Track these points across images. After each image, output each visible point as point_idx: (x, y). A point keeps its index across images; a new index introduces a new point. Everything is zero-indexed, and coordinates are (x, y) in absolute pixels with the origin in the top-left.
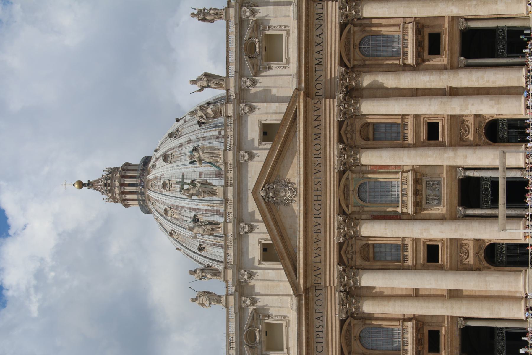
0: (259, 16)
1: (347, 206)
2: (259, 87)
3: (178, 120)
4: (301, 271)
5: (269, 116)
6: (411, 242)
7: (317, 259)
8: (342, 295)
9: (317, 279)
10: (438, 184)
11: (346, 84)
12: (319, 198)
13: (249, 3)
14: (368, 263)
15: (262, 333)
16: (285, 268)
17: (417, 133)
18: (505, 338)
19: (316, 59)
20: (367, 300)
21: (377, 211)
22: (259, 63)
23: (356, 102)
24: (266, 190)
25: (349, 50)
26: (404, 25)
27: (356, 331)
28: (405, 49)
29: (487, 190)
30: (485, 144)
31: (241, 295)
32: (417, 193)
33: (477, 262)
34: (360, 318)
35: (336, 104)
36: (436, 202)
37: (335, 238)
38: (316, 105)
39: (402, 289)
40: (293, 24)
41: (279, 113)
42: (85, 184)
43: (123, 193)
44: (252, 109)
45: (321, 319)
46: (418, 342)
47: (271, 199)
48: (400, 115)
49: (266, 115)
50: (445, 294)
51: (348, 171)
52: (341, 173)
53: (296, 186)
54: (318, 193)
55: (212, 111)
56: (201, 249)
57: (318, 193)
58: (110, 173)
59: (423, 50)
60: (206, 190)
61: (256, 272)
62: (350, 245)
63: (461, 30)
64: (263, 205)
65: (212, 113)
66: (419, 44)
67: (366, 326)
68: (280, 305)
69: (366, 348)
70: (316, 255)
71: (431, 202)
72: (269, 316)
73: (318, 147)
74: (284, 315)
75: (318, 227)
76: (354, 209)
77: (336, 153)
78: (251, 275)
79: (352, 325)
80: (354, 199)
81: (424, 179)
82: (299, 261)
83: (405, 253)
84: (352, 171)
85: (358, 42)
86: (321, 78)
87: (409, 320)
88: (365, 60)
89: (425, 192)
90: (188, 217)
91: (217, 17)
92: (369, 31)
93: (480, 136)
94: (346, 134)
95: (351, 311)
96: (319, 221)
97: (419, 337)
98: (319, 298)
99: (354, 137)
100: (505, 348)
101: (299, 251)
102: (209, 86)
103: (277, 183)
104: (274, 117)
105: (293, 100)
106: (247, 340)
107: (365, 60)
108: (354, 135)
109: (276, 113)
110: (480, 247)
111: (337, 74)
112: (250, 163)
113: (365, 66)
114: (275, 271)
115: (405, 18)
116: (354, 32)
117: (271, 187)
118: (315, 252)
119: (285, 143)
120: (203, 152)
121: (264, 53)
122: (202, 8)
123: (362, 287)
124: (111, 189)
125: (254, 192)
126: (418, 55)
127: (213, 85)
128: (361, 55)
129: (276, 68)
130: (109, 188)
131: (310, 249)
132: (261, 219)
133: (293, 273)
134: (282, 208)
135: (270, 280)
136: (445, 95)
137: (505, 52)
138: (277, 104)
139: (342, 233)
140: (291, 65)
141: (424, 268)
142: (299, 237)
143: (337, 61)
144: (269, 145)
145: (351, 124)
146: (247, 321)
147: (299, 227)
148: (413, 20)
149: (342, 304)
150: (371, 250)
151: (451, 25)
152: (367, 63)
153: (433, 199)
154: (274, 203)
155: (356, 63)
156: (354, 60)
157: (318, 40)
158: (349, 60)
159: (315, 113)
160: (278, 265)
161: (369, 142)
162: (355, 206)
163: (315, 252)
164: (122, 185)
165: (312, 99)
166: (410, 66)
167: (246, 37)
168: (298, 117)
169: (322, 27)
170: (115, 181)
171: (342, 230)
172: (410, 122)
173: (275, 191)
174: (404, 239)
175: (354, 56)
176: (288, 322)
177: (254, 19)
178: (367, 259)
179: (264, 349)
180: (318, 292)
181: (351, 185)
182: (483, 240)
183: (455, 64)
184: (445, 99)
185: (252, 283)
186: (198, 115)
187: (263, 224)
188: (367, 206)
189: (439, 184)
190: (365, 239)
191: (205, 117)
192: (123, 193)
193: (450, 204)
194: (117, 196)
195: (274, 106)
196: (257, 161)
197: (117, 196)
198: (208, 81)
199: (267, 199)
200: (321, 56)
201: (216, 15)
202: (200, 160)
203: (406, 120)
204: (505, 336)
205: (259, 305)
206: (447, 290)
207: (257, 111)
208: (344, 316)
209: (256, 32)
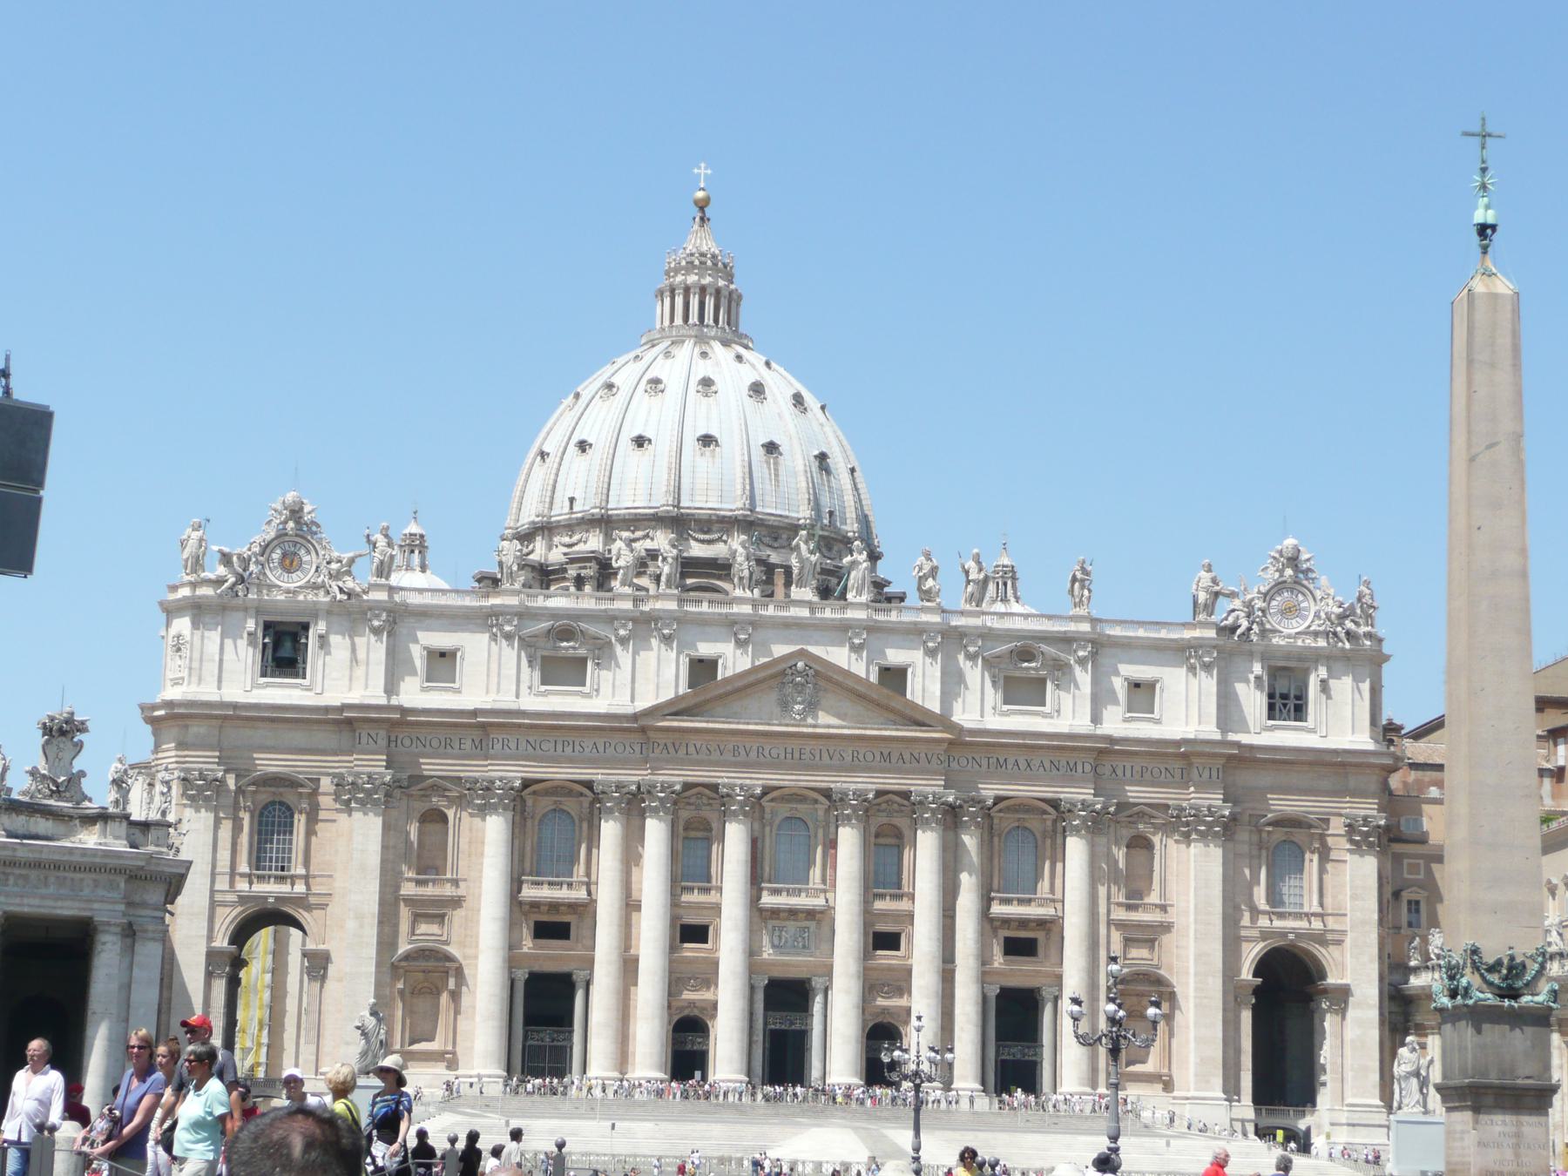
0: (1078, 670)
1: (772, 800)
2: (964, 664)
3: (823, 408)
4: (675, 724)
5: (920, 679)
6: (714, 901)
7: (692, 749)
8: (634, 787)
9: (661, 747)
10: (804, 947)
11: (965, 806)
12: (789, 756)
13: (1097, 653)
14: (681, 828)
15: (571, 651)
16: (678, 699)
17: (884, 915)
18: (555, 1043)
19: (1005, 760)
20: (622, 824)
21: (763, 847)
22: (1002, 666)
23: (938, 822)
24: (805, 670)
25: (1017, 811)
26: (1053, 901)
27: (570, 805)
28: (1015, 902)
29: (792, 1024)
30: (864, 1021)
31: (635, 620)
32: (793, 913)
33: (680, 1004)
34: (591, 813)
35: (937, 789)
36: (776, 942)
37: (726, 780)
38: (935, 757)
39: (641, 883)
40: (1061, 725)
41: (923, 696)
42: (703, 212)
43: (687, 290)
44: (931, 653)
45: (595, 750)
46: (554, 906)
47: (791, 678)
48: (914, 889)
49: (921, 675)
50: (632, 951)
51: (828, 803)
52: (827, 793)
53: (810, 721)
54: (797, 755)
55: (930, 588)
56: (583, 446)
57: (797, 755)
58: (725, 266)
59: (1013, 930)
60: (806, 571)
61: (672, 649)
62: (711, 801)
63: (1039, 989)
64: (784, 666)
65: (927, 586)
66: (1023, 923)
67: (577, 821)
68: (617, 683)
69: (540, 821)
70: (698, 747)
71: (777, 933)
72: (598, 664)
73: (869, 757)
74: (601, 690)
75: (743, 752)
76: (768, 810)
77: (860, 786)
78: (667, 640)
79: (581, 799)
80: (784, 810)
81: (812, 925)
82: (692, 721)
83: (696, 891)
84: (828, 810)
85: (1027, 825)
86: (977, 766)
87: (589, 893)
88: (1000, 836)
89: (792, 926)
90: (645, 425)
91: (1077, 600)
92: (1044, 842)
93: (878, 1015)
94: (887, 802)
95: (605, 800)
96: (753, 755)
97: (562, 908)
98: (628, 748)
99: (881, 814)
100: (540, 1043)
101: (707, 722)
102: (968, 582)
103: (815, 688)
104: (918, 687)
105: (944, 721)
106: (560, 626)
107: (1000, 836)
108: (885, 814)
109: (924, 690)
110: (703, 1009)
111: (984, 792)
112: (846, 650)
113: (991, 836)
114: (674, 678)
115: (1063, 902)
116: (1045, 820)
117: (809, 680)
118: (704, 746)
119: (878, 705)
120: (866, 569)
121: (1017, 674)
122: (1093, 577)
123: (645, 819)
124: (695, 267)
125: (802, 654)
126: (1006, 922)
127: (970, 589)
128: (1007, 830)
129: (993, 696)
130: (697, 262)
131: (707, 738)
132: (757, 663)
133: (674, 709)
134: (774, 696)
135: (658, 670)
136: (944, 962)
137: (1004, 1057)
138: (938, 693)
139: (734, 790)
140: (998, 718)
141: (674, 919)
142: (730, 723)
143: (1001, 793)
144: (874, 678)
145: (902, 811)
146: (592, 629)
147: (744, 723)
148: (1060, 914)
149: (619, 786)
150: (700, 834)
151: (1048, 975)
152: (996, 839)
153: (780, 937)
154: (784, 683)
155: (996, 821)
156: (1001, 818)
157: (1036, 763)
158: (1000, 811)
159: (923, 755)
160: (683, 689)
161: (873, 839)
162: (772, 813)
163: (704, 746)
164: (703, 290)
165: (945, 751)
166: (989, 909)
167: (1044, 647)
168: (918, 728)
169: (1055, 771)
170: (709, 275)
171: (738, 791)
172: (903, 905)
173: (803, 685)
174: (720, 889)
175: (1007, 818)
176: (587, 696)
177: (1072, 662)
178: (686, 829)
179: (546, 653)
180: (637, 748)
181: (806, 806)
182: (714, 1016)
183: (988, 979)
184: (938, 962)
185: (654, 642)
186: (925, 562)
187: (749, 666)
188: (771, 831)
189: (804, 947)
190: (721, 827)
191: (921, 574)
192: (687, 290)
193: (773, 964)
194: (679, 278)
195: (936, 688)
196: (849, 657)
197: (679, 278)
198: (976, 582)
199: (790, 672)
200: (1010, 767)
201: (1081, 600)
202: (854, 564)
203: (905, 899)
204: (559, 1044)
205: (618, 649)
206: (638, 956)
207: (928, 660)
208: (598, 788)
209: (1051, 663)
